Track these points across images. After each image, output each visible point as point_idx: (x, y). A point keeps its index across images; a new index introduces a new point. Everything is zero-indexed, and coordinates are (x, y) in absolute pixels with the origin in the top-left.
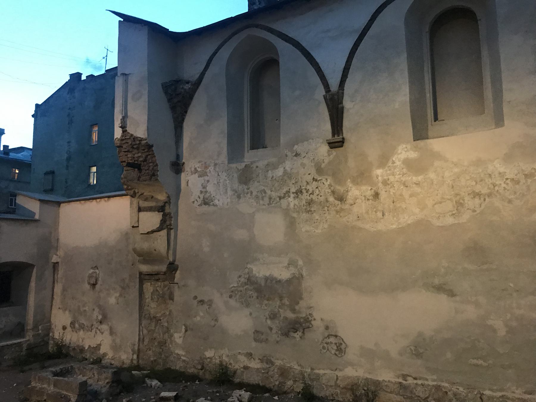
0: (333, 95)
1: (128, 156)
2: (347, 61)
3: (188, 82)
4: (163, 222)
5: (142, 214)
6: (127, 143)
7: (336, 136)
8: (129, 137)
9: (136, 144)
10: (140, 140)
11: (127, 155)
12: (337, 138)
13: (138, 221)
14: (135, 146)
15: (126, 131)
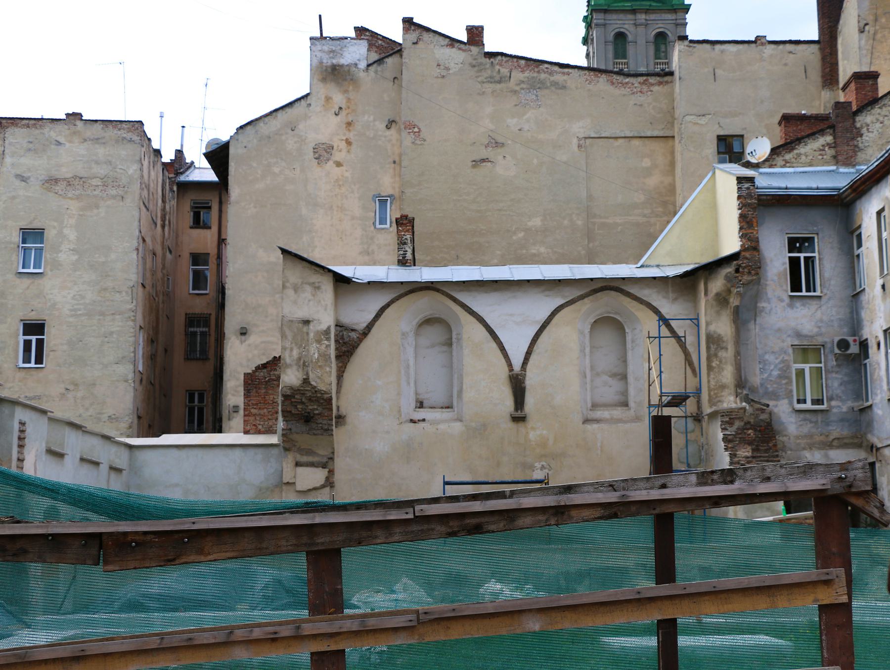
0: (517, 375)
1: (298, 406)
2: (529, 347)
3: (353, 330)
4: (327, 478)
5: (300, 470)
6: (303, 394)
7: (519, 411)
8: (309, 389)
9: (316, 396)
10: (322, 394)
11: (296, 406)
12: (519, 414)
13: (295, 477)
14: (314, 399)
15: (309, 382)
